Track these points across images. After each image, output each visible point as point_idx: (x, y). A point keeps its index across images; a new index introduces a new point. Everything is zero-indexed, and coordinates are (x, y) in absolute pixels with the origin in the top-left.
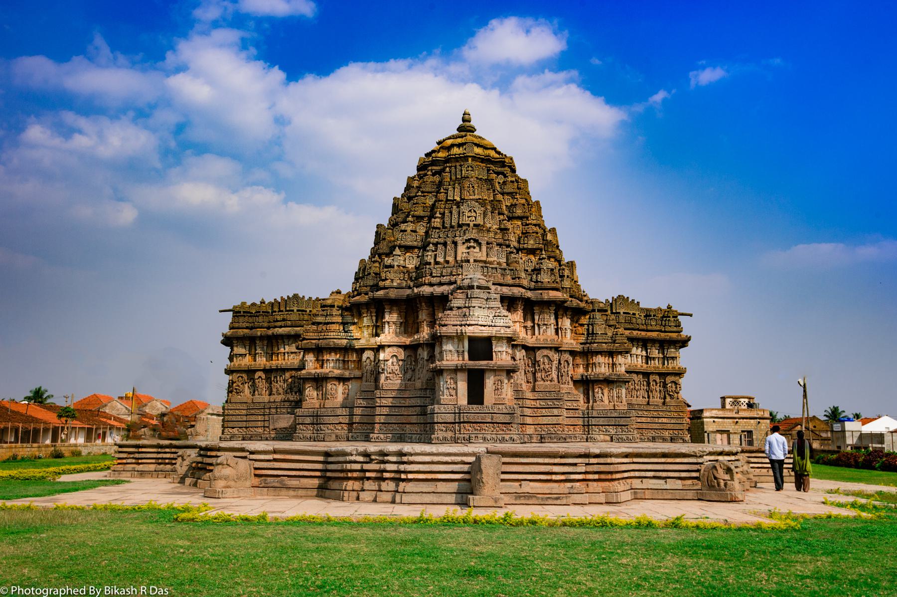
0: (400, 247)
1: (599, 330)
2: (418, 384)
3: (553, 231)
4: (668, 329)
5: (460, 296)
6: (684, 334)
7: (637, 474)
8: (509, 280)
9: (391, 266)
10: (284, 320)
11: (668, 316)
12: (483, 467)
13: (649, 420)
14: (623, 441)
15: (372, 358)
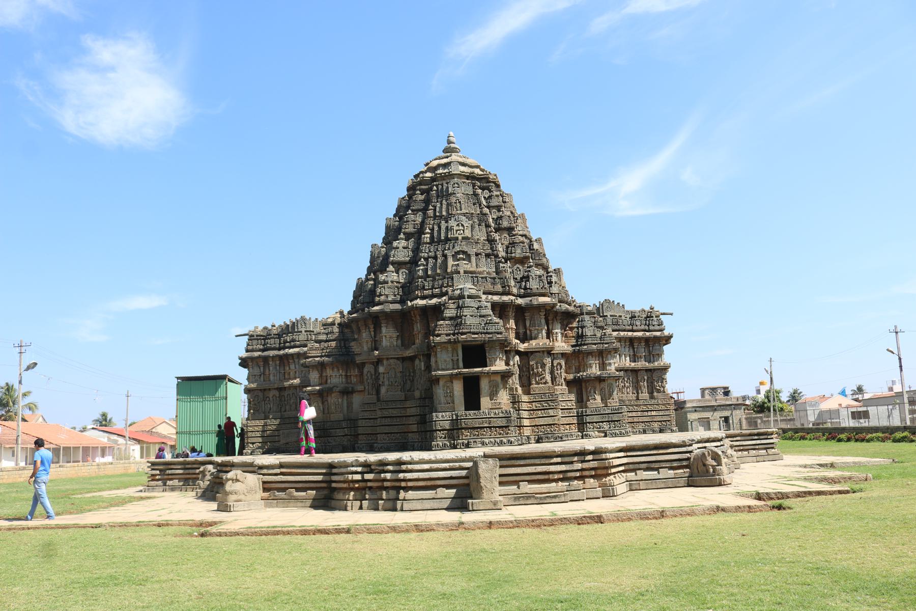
0: (393, 263)
1: (588, 332)
2: (417, 394)
3: (539, 241)
4: (651, 328)
5: (452, 306)
6: (666, 333)
7: (631, 467)
8: (499, 288)
9: (386, 282)
10: (293, 340)
11: (650, 318)
12: (480, 471)
13: (639, 414)
14: (616, 435)
15: (373, 372)
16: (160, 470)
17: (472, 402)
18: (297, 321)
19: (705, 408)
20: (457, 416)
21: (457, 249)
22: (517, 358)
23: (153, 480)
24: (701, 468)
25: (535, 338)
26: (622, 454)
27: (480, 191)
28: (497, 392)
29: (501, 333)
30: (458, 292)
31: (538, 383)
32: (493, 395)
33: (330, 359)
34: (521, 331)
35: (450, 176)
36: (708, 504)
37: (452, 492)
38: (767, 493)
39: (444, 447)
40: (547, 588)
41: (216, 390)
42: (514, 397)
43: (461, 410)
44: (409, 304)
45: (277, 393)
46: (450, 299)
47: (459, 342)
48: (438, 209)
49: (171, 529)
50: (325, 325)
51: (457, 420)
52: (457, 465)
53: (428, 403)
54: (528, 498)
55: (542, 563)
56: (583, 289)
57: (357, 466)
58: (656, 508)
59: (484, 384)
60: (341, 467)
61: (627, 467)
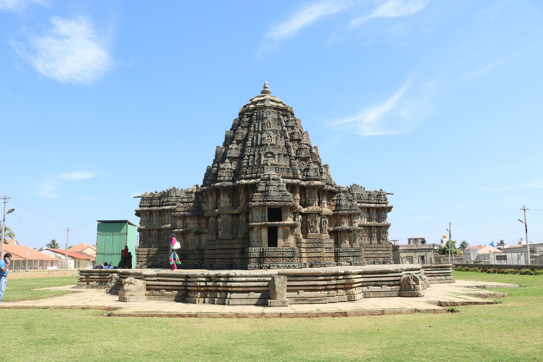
0: (229, 158)
1: (343, 203)
2: (240, 236)
3: (316, 148)
4: (380, 202)
5: (263, 184)
6: (389, 205)
7: (365, 284)
8: (291, 175)
10: (168, 201)
11: (380, 196)
12: (276, 283)
13: (371, 252)
14: (357, 265)
15: (214, 222)
16: (86, 276)
17: (273, 242)
18: (171, 190)
19: (410, 250)
20: (263, 249)
21: (267, 150)
22: (300, 217)
23: (81, 281)
24: (407, 286)
25: (312, 205)
26: (360, 276)
27: (282, 117)
28: (287, 237)
29: (291, 202)
30: (267, 176)
31: (312, 232)
32: (285, 238)
33: (189, 213)
34: (303, 201)
35: (265, 107)
36: (410, 307)
37: (259, 295)
38: (445, 302)
39: (255, 268)
40: (313, 354)
41: (121, 229)
42: (297, 240)
43: (266, 247)
44: (238, 182)
45: (157, 232)
46: (262, 180)
47: (266, 206)
48: (256, 127)
50: (187, 193)
51: (263, 252)
52: (262, 279)
53: (246, 242)
55: (310, 339)
56: (341, 177)
57: (203, 277)
58: (379, 308)
59: (280, 232)
61: (363, 284)
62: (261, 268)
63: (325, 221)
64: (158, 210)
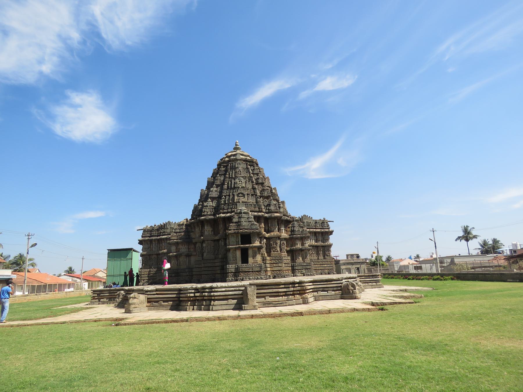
0: (210, 198)
1: (296, 229)
2: (220, 256)
3: (275, 189)
5: (236, 217)
6: (331, 230)
7: (315, 290)
8: (257, 209)
9: (207, 206)
10: (164, 232)
11: (324, 223)
12: (248, 291)
14: (309, 275)
16: (97, 294)
17: (245, 260)
19: (348, 264)
21: (239, 192)
22: (265, 240)
24: (347, 290)
25: (273, 232)
26: (311, 284)
28: (256, 256)
31: (274, 252)
32: (254, 257)
34: (267, 228)
35: (236, 160)
36: (350, 307)
40: (277, 347)
41: (127, 255)
42: (263, 258)
43: (240, 264)
45: (156, 256)
49: (101, 323)
50: (179, 225)
53: (225, 261)
54: (269, 304)
55: (275, 335)
56: (294, 210)
58: (326, 309)
59: (250, 252)
60: (185, 290)
61: (314, 290)
62: (237, 280)
63: (283, 243)
64: (157, 239)
